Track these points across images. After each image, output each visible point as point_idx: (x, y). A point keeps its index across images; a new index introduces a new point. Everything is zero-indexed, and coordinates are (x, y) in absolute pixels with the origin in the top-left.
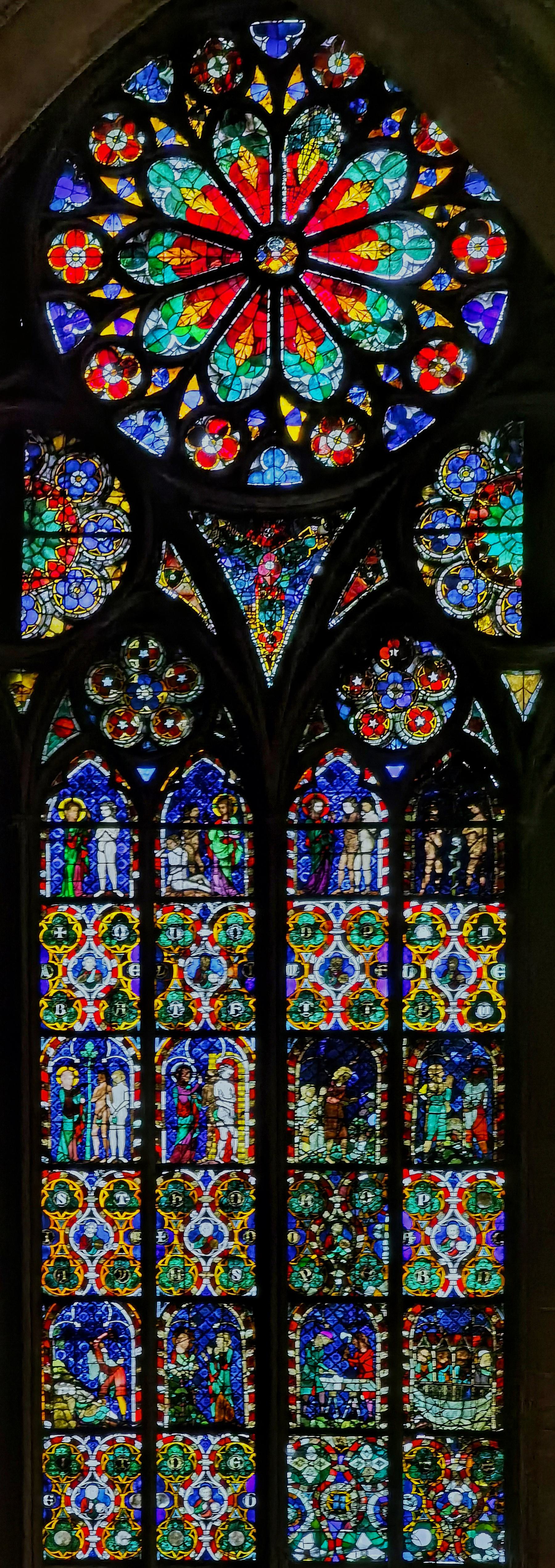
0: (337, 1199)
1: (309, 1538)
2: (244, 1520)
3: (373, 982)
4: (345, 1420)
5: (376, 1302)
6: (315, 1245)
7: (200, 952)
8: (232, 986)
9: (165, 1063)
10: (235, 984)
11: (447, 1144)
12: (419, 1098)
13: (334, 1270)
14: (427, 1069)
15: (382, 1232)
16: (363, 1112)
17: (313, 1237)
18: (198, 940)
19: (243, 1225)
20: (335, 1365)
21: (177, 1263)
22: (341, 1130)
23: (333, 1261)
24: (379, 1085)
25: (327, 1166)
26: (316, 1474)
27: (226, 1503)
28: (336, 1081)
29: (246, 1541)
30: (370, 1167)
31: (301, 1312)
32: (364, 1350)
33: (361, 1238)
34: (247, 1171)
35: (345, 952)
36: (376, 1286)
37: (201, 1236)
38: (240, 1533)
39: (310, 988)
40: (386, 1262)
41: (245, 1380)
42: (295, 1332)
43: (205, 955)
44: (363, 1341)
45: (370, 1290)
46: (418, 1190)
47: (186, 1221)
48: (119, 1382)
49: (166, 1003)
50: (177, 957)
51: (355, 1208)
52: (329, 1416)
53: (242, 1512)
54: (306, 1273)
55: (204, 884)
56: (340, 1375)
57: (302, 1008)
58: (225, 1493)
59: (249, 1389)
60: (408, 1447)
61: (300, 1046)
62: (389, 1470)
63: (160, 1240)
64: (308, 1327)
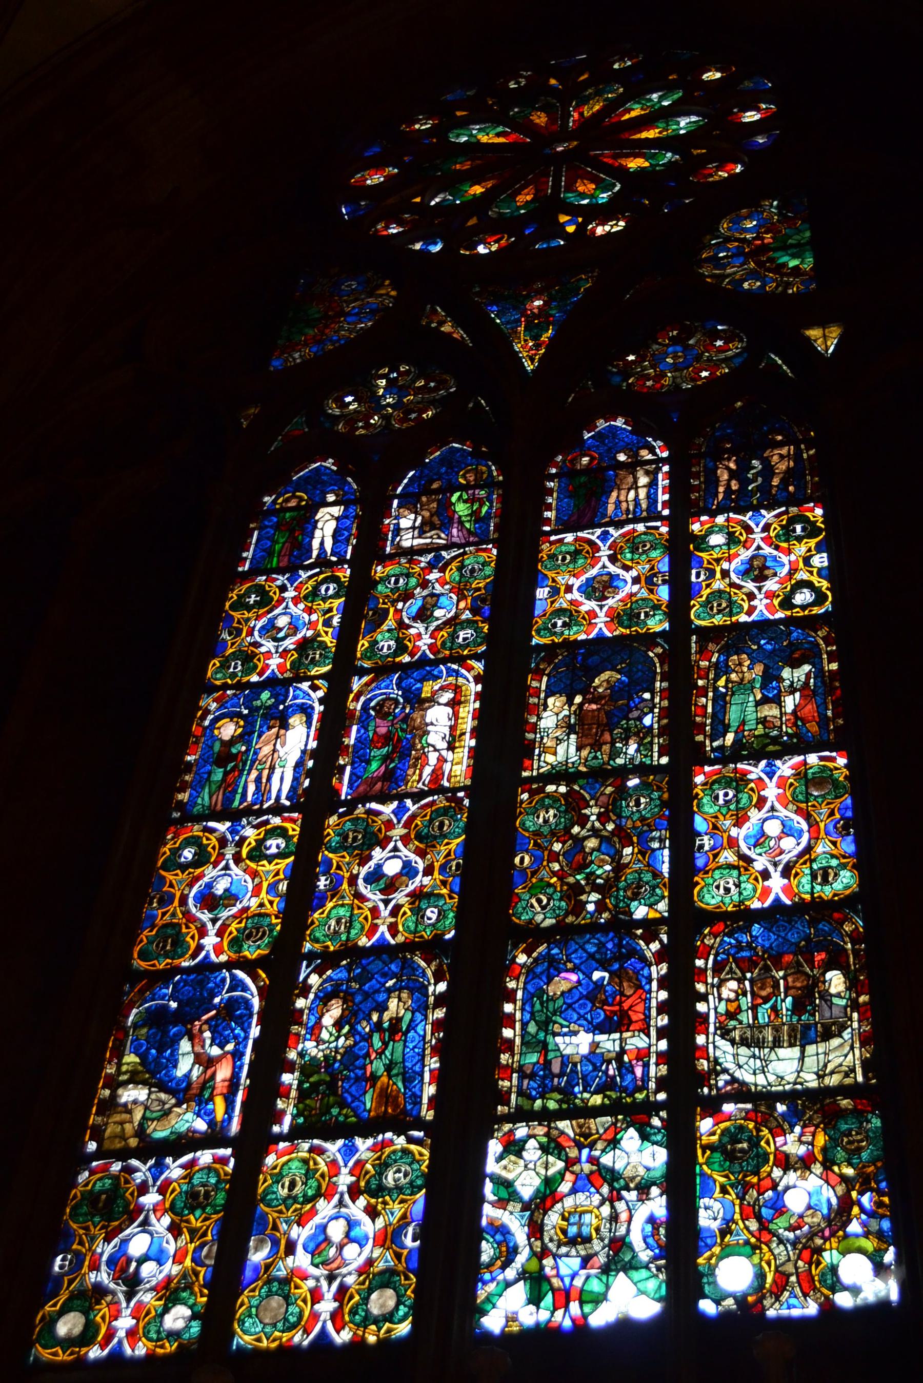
0: (592, 812)
1: (520, 1291)
2: (400, 1268)
3: (651, 591)
4: (596, 1092)
5: (650, 928)
6: (556, 867)
7: (425, 593)
8: (464, 617)
9: (362, 699)
10: (467, 615)
11: (760, 730)
12: (716, 689)
13: (584, 892)
14: (727, 661)
15: (661, 840)
16: (636, 714)
17: (554, 857)
18: (424, 584)
19: (449, 854)
20: (581, 1017)
21: (342, 912)
22: (602, 734)
23: (583, 882)
24: (658, 684)
25: (578, 775)
26: (537, 1182)
27: (371, 1242)
28: (595, 688)
29: (398, 1303)
30: (642, 770)
31: (529, 953)
32: (628, 992)
33: (628, 851)
34: (461, 794)
35: (612, 569)
36: (650, 906)
37: (384, 875)
38: (390, 1292)
39: (565, 605)
40: (667, 875)
41: (428, 1052)
42: (518, 980)
43: (432, 595)
44: (629, 980)
45: (640, 912)
46: (716, 786)
47: (364, 861)
48: (223, 1072)
49: (374, 643)
50: (394, 602)
51: (620, 817)
52: (567, 1093)
53: (398, 1256)
54: (539, 901)
55: (439, 538)
56: (587, 1031)
57: (555, 624)
58: (368, 1227)
59: (433, 1063)
60: (705, 1125)
61: (549, 660)
62: (671, 1164)
63: (322, 887)
64: (539, 970)
